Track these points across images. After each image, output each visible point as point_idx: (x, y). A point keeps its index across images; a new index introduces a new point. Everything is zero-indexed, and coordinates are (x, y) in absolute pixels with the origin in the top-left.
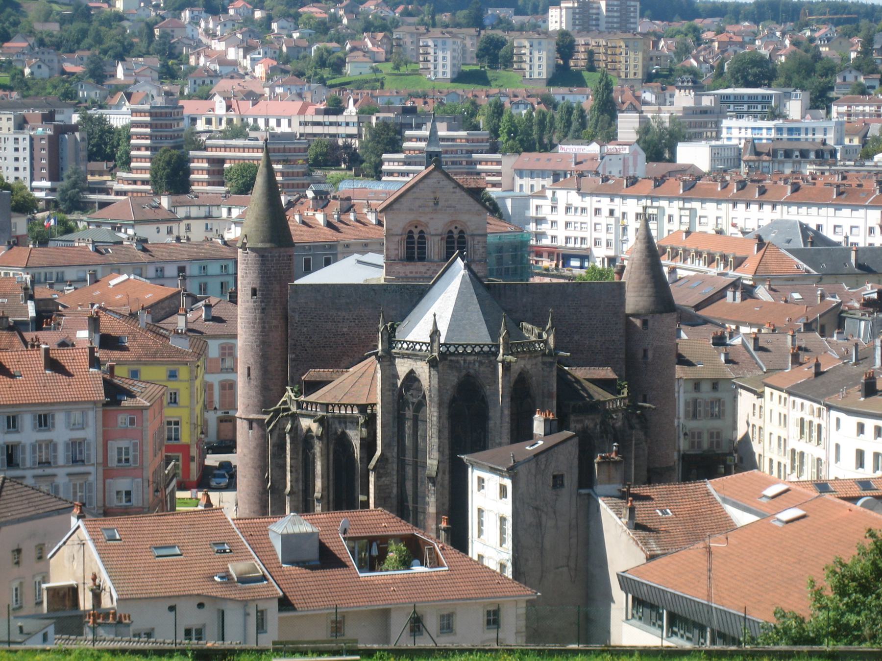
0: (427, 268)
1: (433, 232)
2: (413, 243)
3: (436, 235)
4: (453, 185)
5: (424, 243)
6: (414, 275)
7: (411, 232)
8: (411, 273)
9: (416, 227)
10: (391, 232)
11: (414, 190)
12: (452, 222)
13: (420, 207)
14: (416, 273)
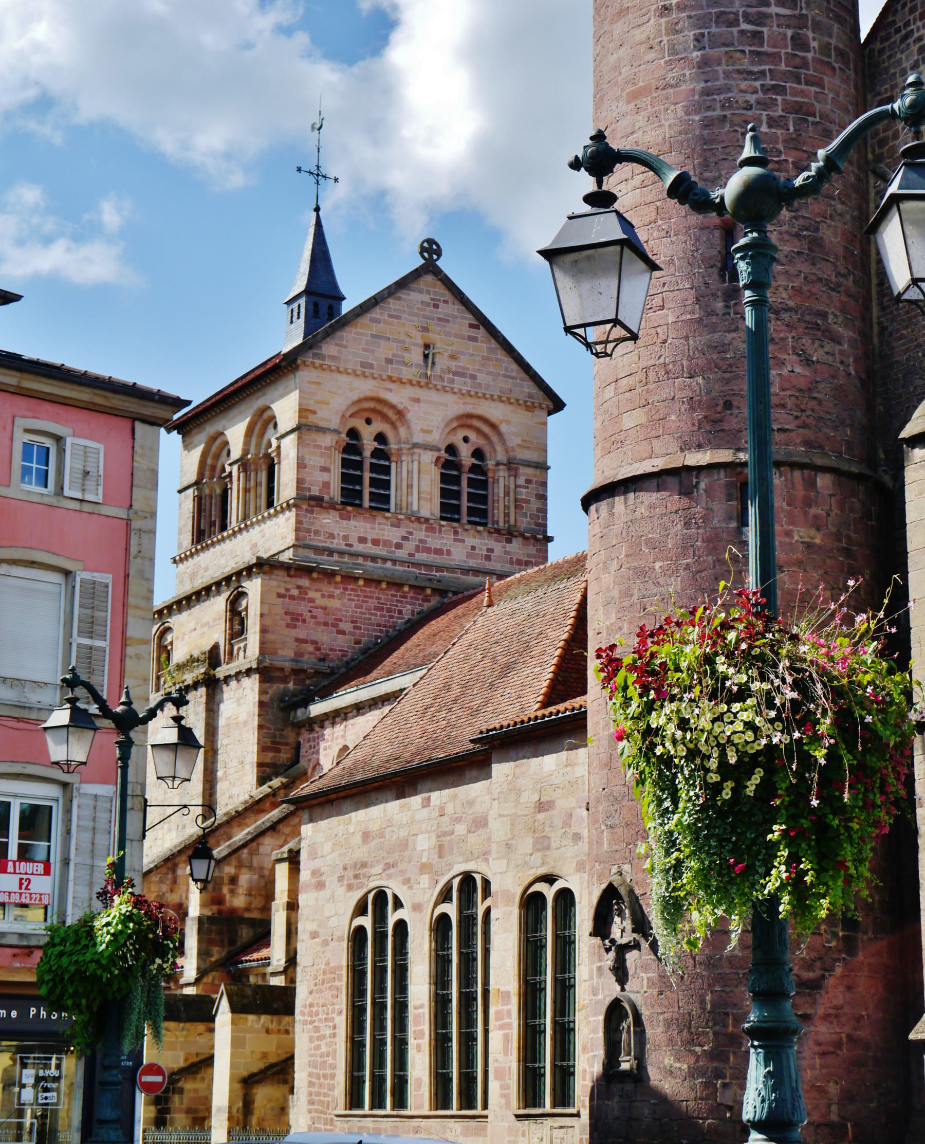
0: (402, 532)
1: (418, 438)
2: (359, 465)
3: (426, 447)
4: (470, 318)
5: (387, 470)
6: (368, 548)
7: (353, 433)
8: (362, 540)
9: (368, 421)
10: (312, 419)
11: (376, 313)
12: (465, 420)
13: (389, 361)
14: (376, 542)
